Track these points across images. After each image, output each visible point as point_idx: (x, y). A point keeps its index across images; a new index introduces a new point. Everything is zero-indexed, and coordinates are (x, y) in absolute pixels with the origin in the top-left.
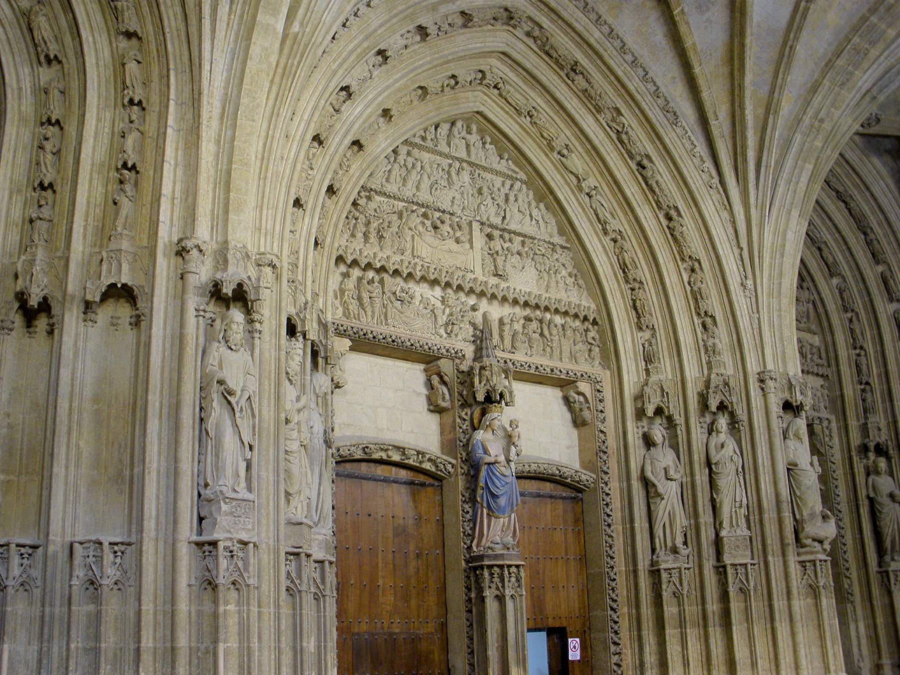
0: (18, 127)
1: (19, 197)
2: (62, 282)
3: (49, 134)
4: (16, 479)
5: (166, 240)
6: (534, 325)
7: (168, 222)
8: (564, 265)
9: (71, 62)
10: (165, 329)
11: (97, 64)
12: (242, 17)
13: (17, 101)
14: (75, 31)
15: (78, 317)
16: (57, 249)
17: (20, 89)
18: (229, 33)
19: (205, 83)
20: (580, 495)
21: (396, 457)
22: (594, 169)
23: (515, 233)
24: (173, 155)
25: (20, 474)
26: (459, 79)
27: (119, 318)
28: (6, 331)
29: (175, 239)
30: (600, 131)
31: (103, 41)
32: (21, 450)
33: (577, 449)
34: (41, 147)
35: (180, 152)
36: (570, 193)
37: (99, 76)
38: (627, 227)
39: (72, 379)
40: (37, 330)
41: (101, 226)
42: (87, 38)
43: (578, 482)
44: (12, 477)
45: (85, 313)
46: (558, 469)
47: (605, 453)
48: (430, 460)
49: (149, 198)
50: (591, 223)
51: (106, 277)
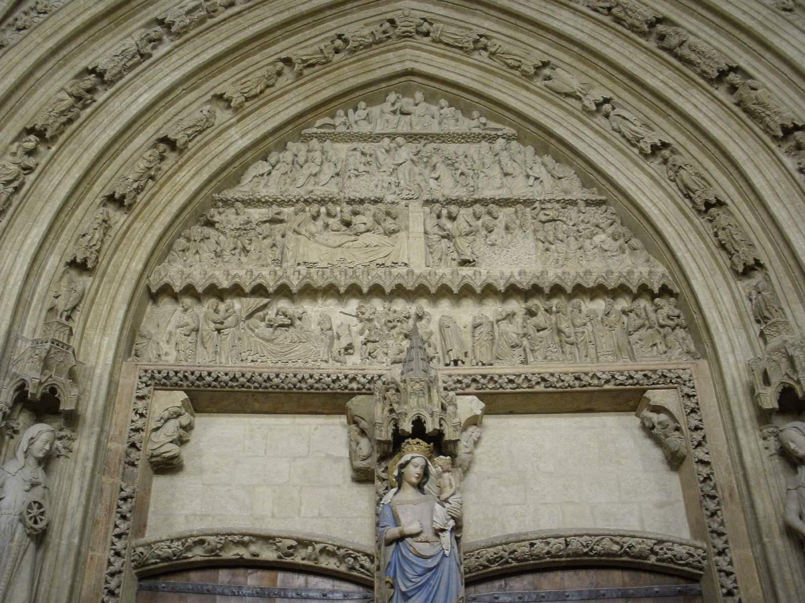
6: (541, 319)
8: (597, 226)
20: (696, 586)
21: (269, 555)
22: (599, 77)
23: (495, 202)
26: (347, 36)
30: (586, 23)
33: (681, 505)
36: (579, 125)
38: (674, 133)
43: (671, 560)
46: (617, 543)
47: (713, 497)
48: (323, 551)
50: (620, 150)
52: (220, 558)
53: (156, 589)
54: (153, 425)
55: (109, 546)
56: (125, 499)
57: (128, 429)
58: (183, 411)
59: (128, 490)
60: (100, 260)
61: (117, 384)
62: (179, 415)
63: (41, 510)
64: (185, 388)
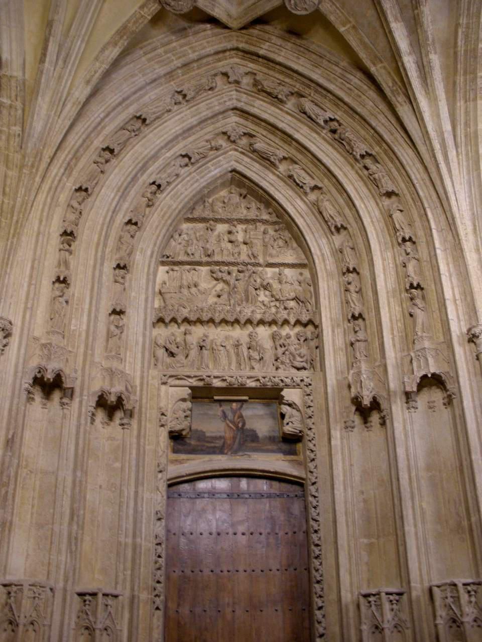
0: (328, 281)
1: (339, 330)
2: (385, 382)
3: (350, 279)
4: (376, 541)
5: (458, 333)
7: (456, 319)
9: (353, 227)
10: (473, 401)
11: (372, 221)
12: (467, 155)
13: (322, 264)
14: (351, 204)
15: (402, 407)
16: (375, 360)
17: (323, 255)
18: (461, 170)
19: (455, 209)
24: (446, 268)
25: (379, 537)
27: (434, 402)
28: (350, 429)
29: (465, 330)
31: (372, 204)
32: (377, 517)
34: (347, 290)
35: (451, 266)
37: (375, 229)
39: (407, 455)
40: (372, 424)
41: (404, 335)
42: (360, 206)
44: (373, 540)
45: (407, 403)
49: (437, 306)
51: (418, 371)
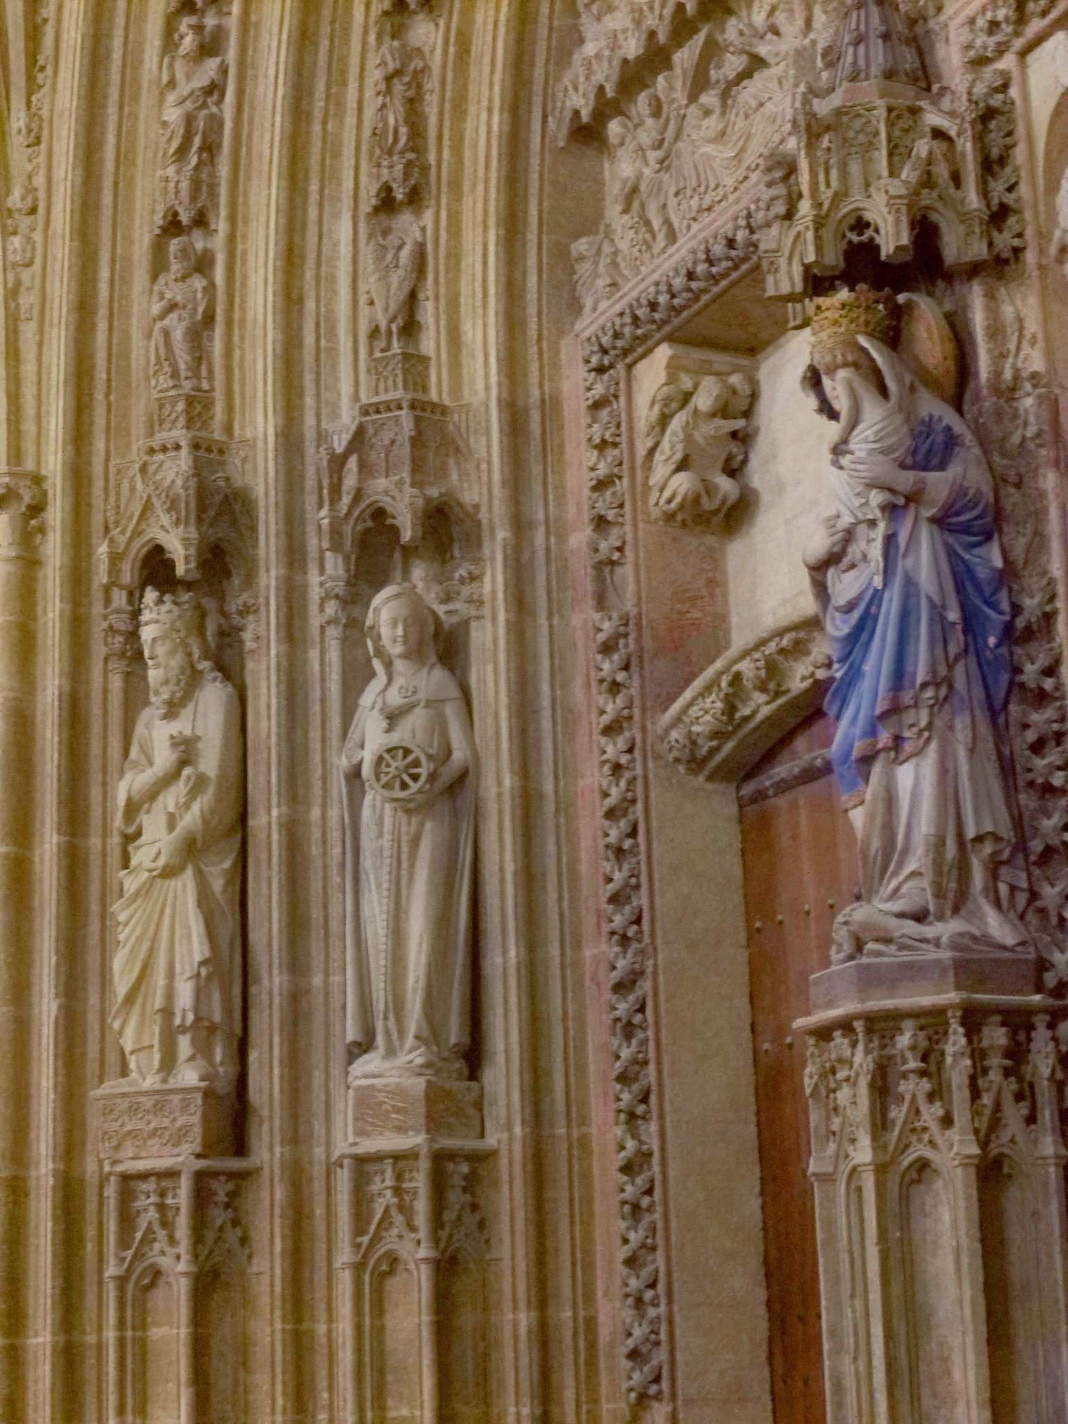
52: (790, 695)
53: (760, 796)
54: (641, 452)
55: (596, 759)
56: (607, 648)
57: (586, 492)
58: (687, 382)
59: (606, 625)
60: (432, 158)
61: (552, 406)
62: (687, 397)
63: (410, 758)
64: (657, 336)
